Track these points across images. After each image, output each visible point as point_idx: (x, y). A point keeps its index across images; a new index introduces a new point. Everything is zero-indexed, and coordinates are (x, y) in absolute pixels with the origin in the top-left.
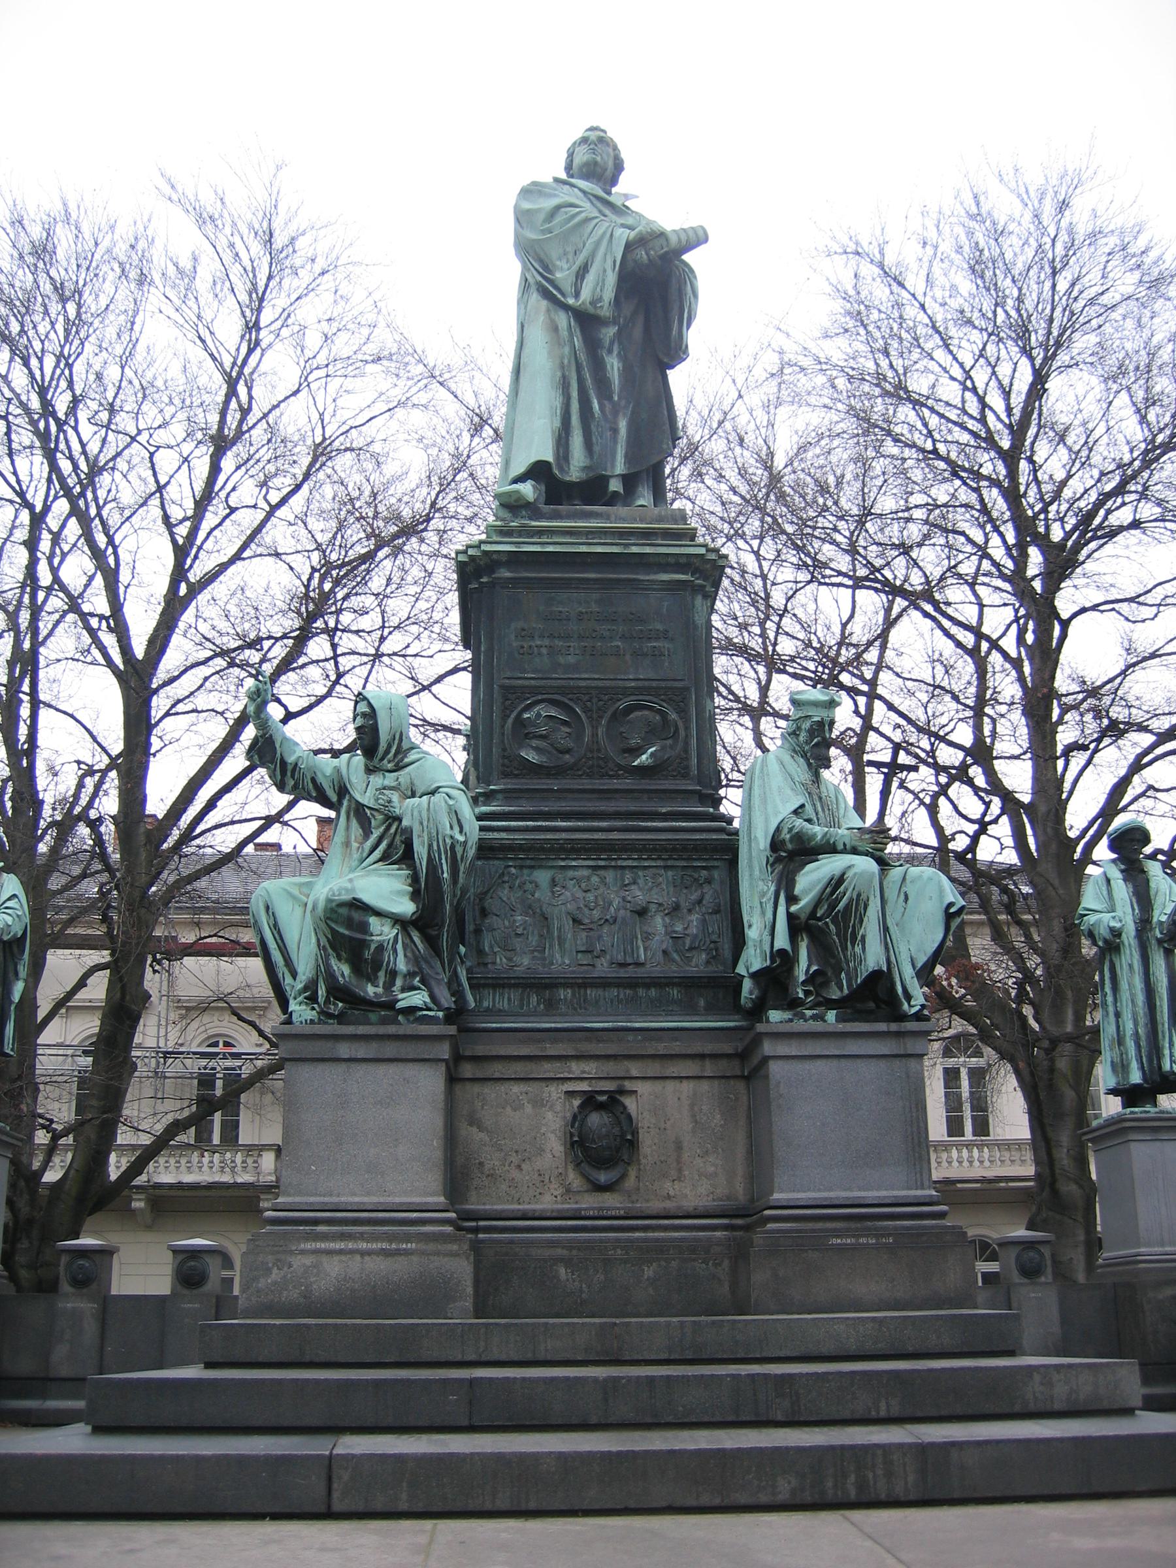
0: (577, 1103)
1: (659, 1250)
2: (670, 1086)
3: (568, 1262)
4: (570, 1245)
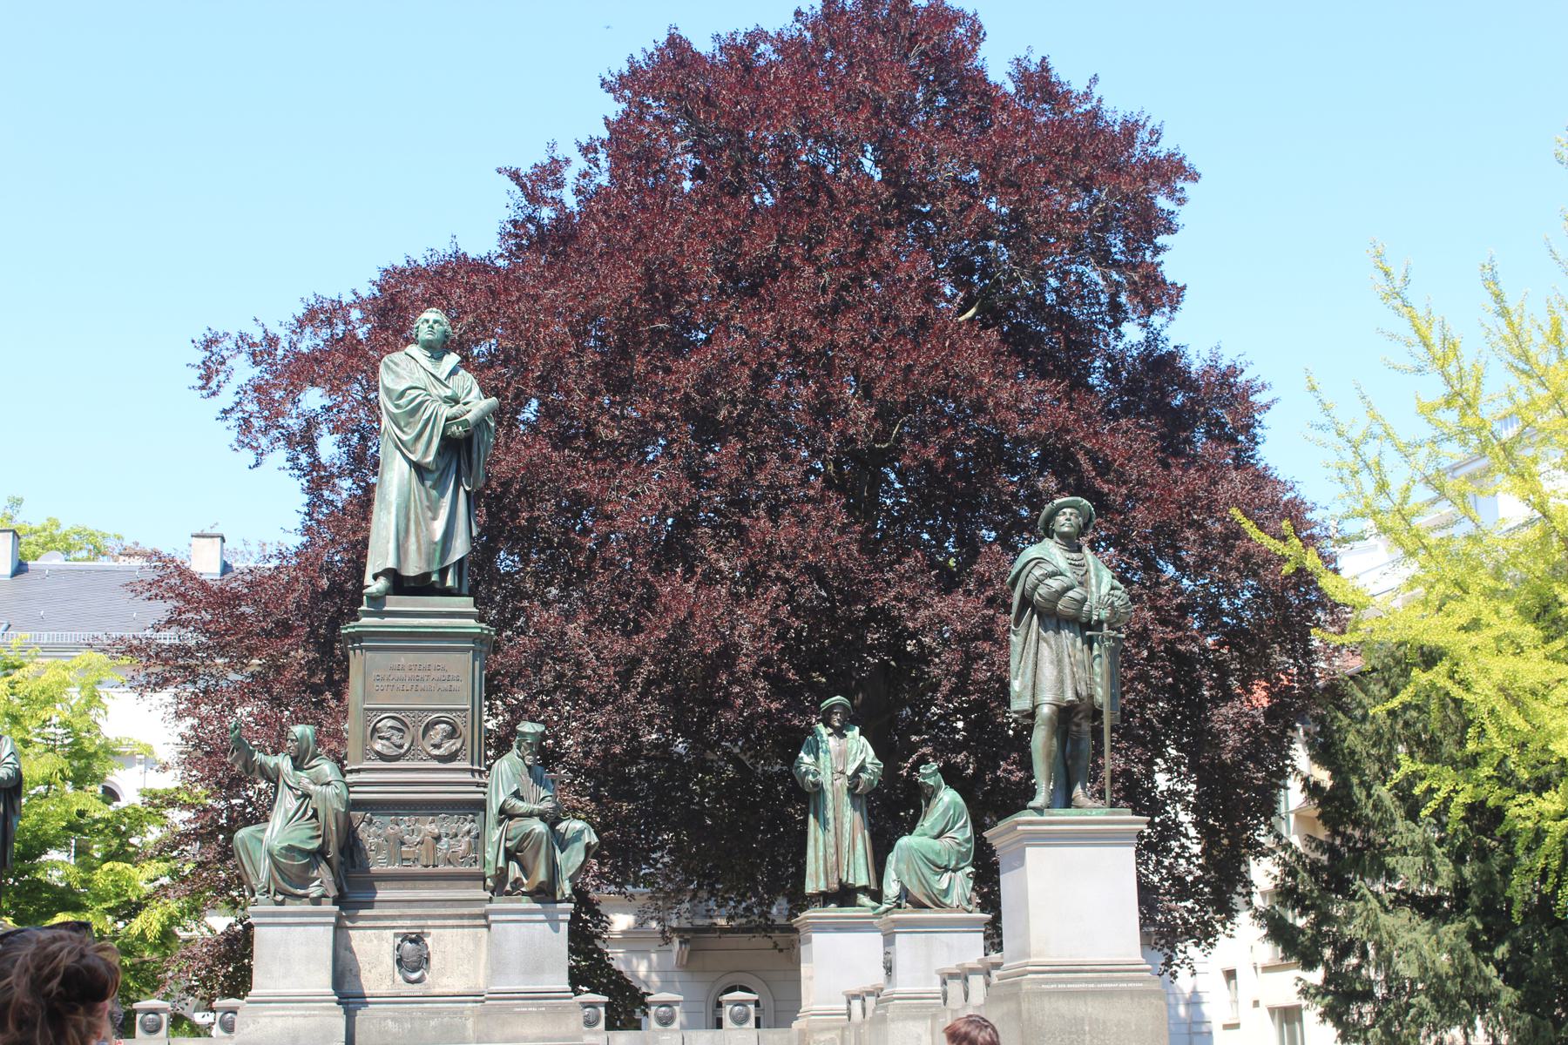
1: (438, 1012)
3: (394, 1019)
4: (394, 1010)
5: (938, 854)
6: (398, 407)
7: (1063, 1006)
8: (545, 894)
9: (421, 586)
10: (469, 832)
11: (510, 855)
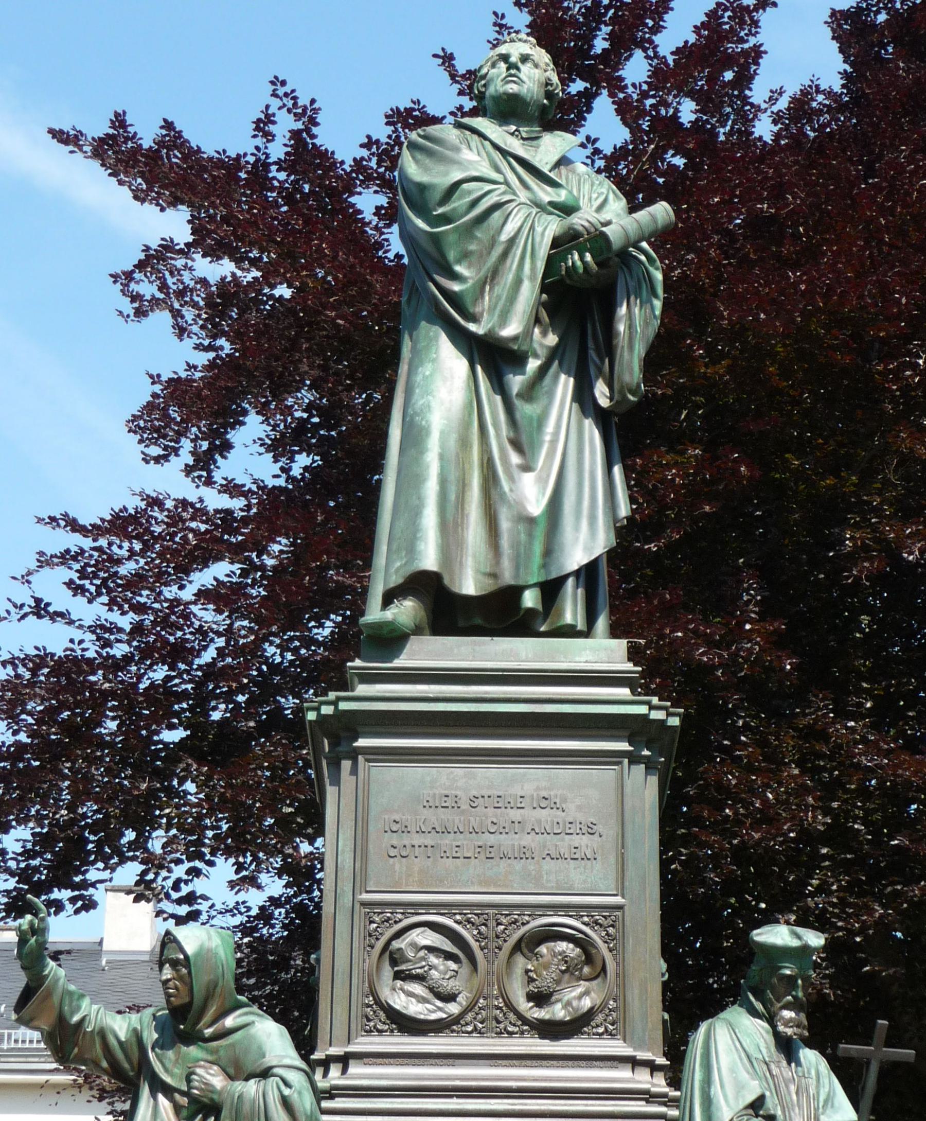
9: (500, 614)
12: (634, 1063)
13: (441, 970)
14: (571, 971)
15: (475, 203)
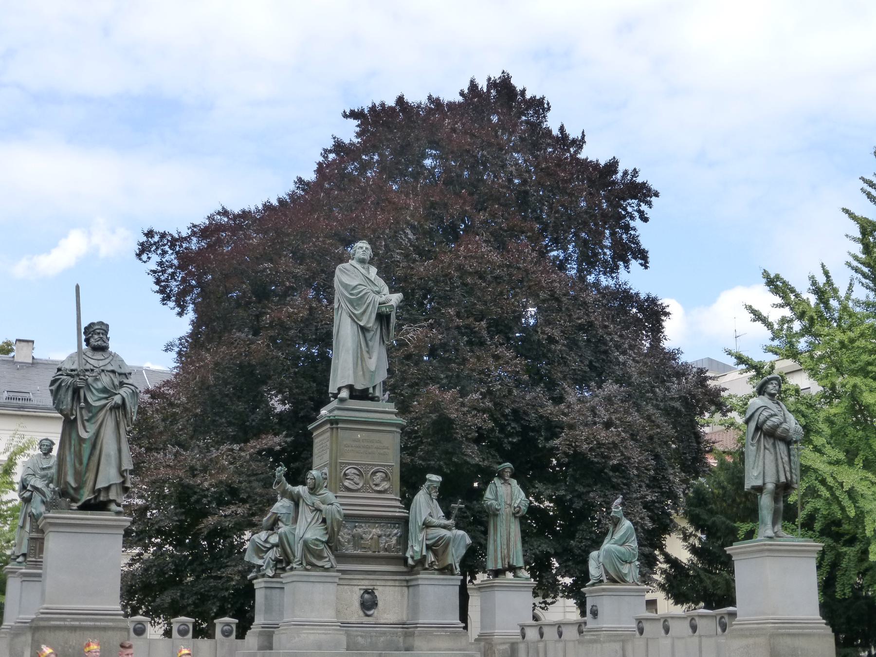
0: (362, 592)
1: (384, 633)
2: (387, 588)
3: (361, 636)
4: (363, 632)
5: (623, 554)
6: (351, 294)
7: (789, 641)
8: (447, 570)
10: (396, 534)
11: (429, 547)
12: (396, 500)
13: (356, 479)
14: (383, 480)
15: (360, 292)
